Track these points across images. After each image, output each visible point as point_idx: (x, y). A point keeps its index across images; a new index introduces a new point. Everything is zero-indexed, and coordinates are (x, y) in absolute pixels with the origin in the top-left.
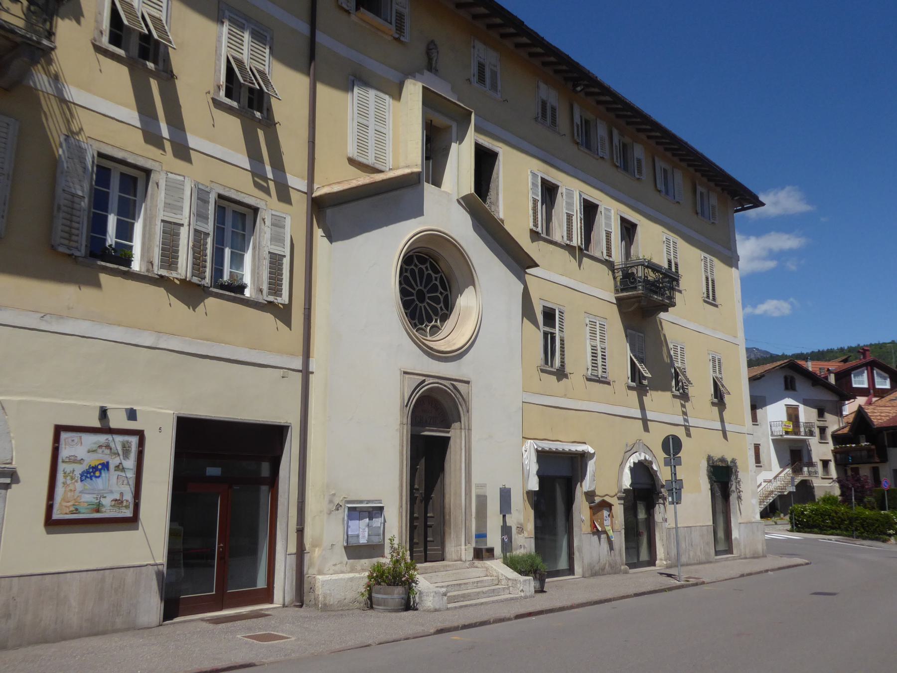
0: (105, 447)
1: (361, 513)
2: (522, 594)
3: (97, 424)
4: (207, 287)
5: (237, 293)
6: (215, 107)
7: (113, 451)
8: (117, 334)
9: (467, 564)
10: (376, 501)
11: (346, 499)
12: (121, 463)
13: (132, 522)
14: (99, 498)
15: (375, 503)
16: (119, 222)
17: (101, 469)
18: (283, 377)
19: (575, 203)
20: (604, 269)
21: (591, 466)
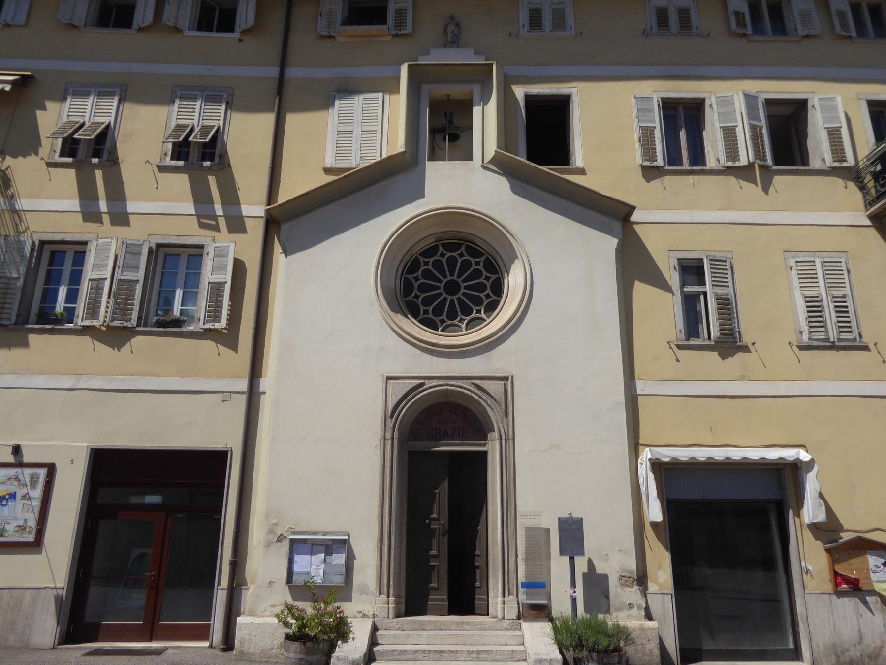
0: (14, 479)
1: (314, 547)
3: (11, 459)
4: (132, 327)
5: (167, 328)
6: (160, 172)
7: (20, 482)
8: (40, 381)
9: (505, 624)
11: (293, 530)
12: (28, 493)
13: (37, 545)
14: (3, 524)
15: (337, 535)
16: (69, 290)
17: (8, 499)
18: (223, 401)
19: (737, 110)
20: (838, 182)
21: (811, 484)
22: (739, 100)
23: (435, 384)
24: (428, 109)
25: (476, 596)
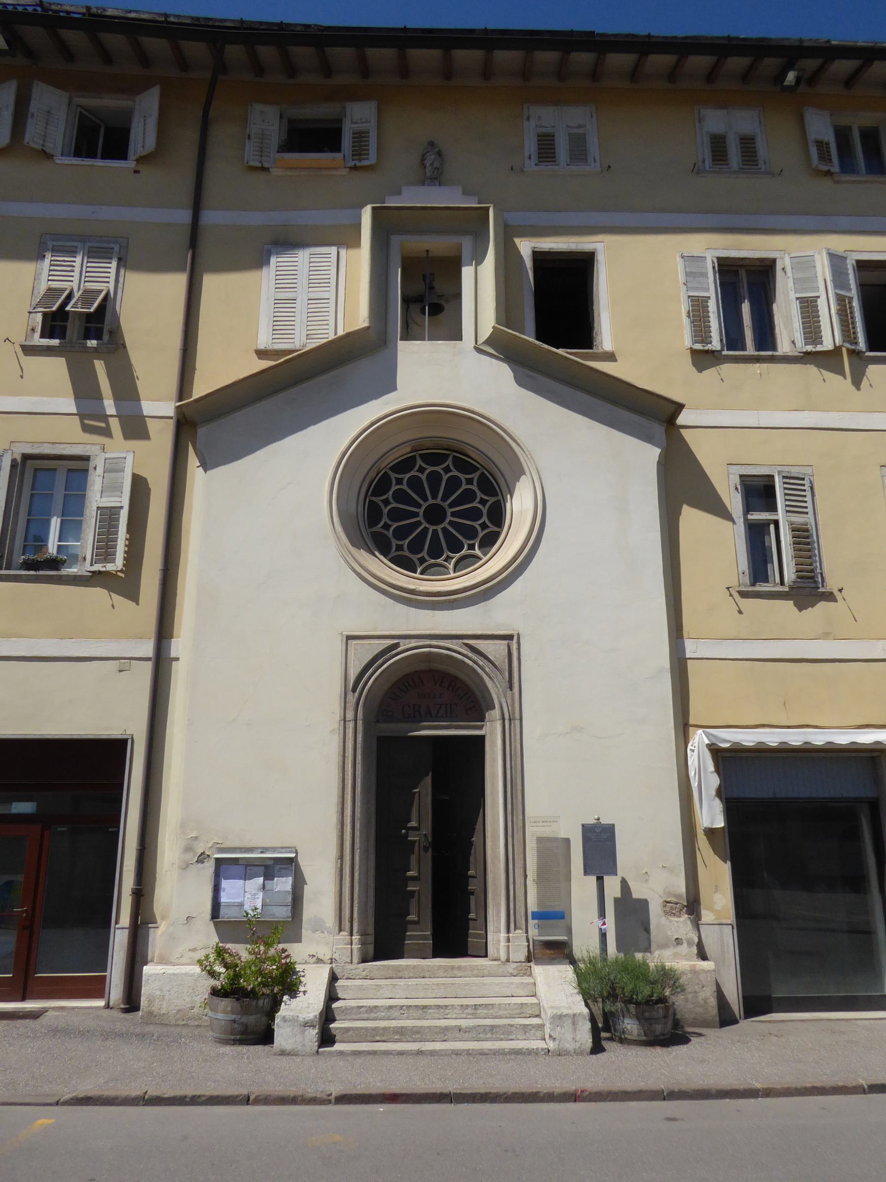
2: (552, 1045)
5: (39, 570)
6: (25, 355)
9: (511, 968)
10: (282, 848)
11: (218, 846)
18: (120, 671)
22: (823, 262)
24: (400, 269)
25: (470, 931)
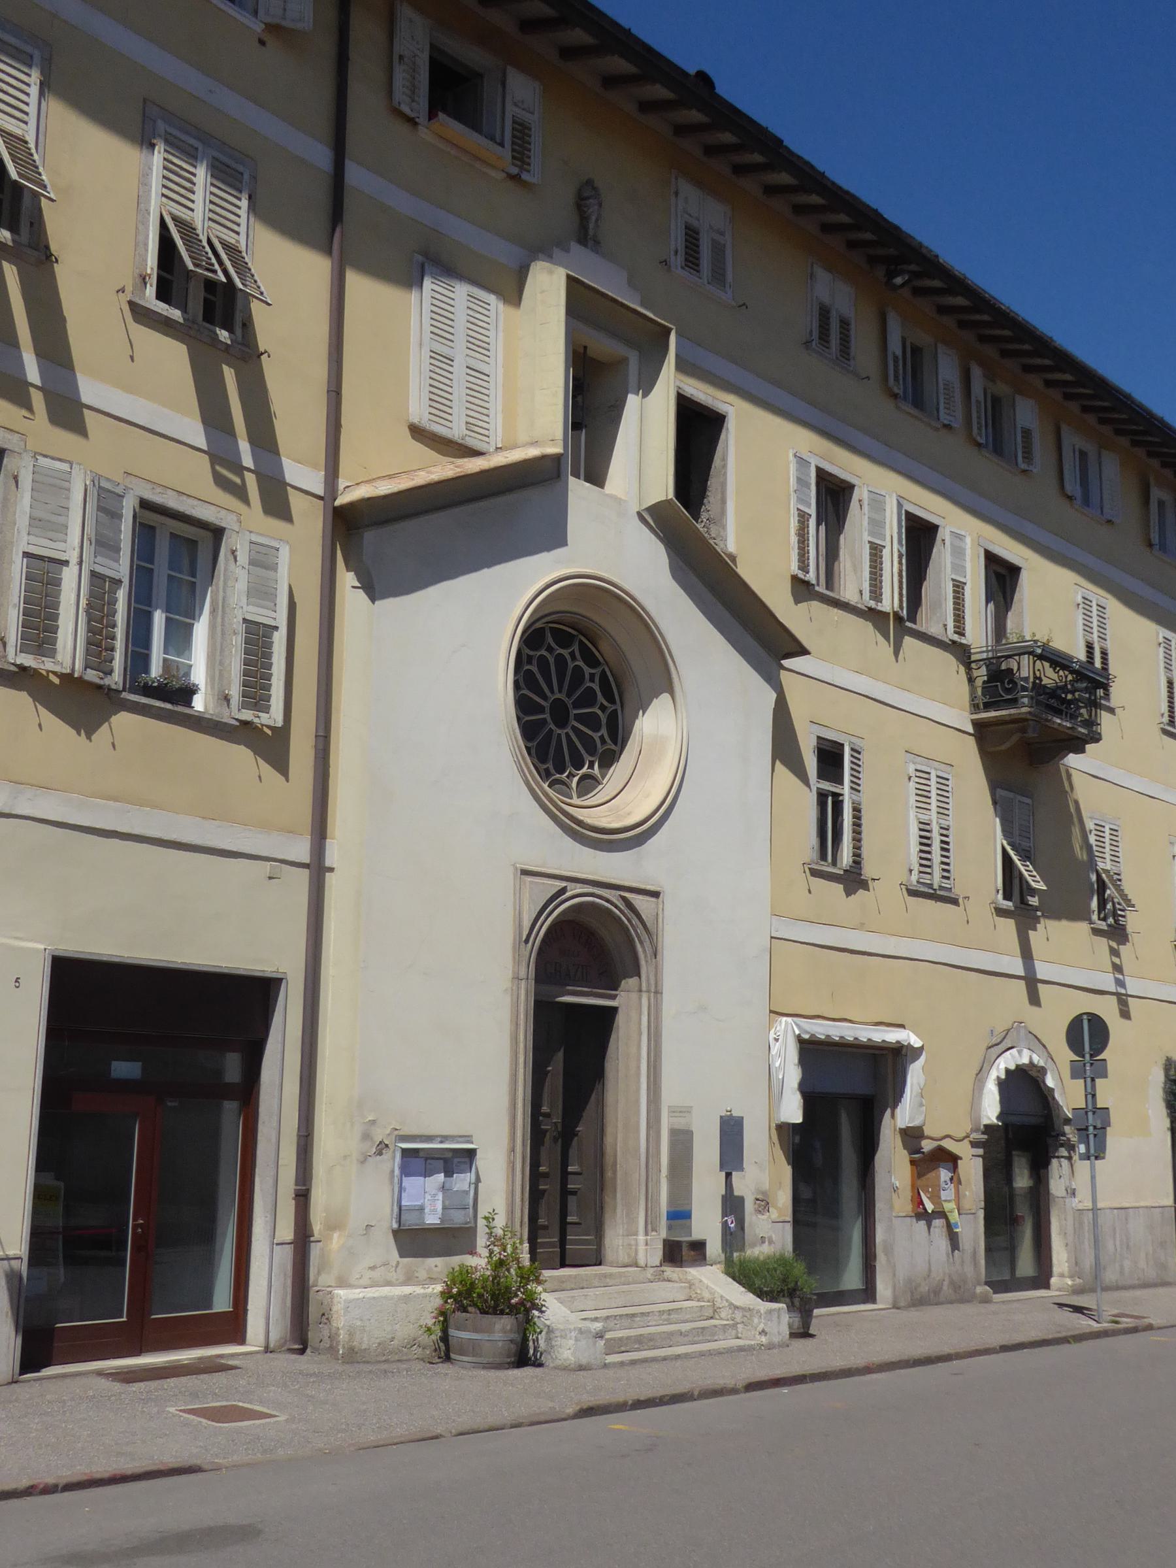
2: (764, 1339)
6: (136, 320)
9: (649, 1273)
10: (460, 1136)
15: (458, 1142)
18: (270, 878)
21: (915, 1075)
22: (892, 512)
23: (579, 891)
24: (571, 369)
25: (539, 1241)
